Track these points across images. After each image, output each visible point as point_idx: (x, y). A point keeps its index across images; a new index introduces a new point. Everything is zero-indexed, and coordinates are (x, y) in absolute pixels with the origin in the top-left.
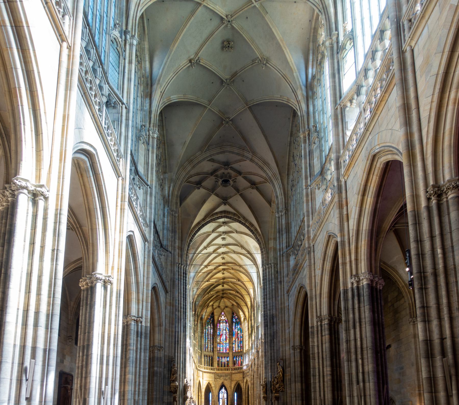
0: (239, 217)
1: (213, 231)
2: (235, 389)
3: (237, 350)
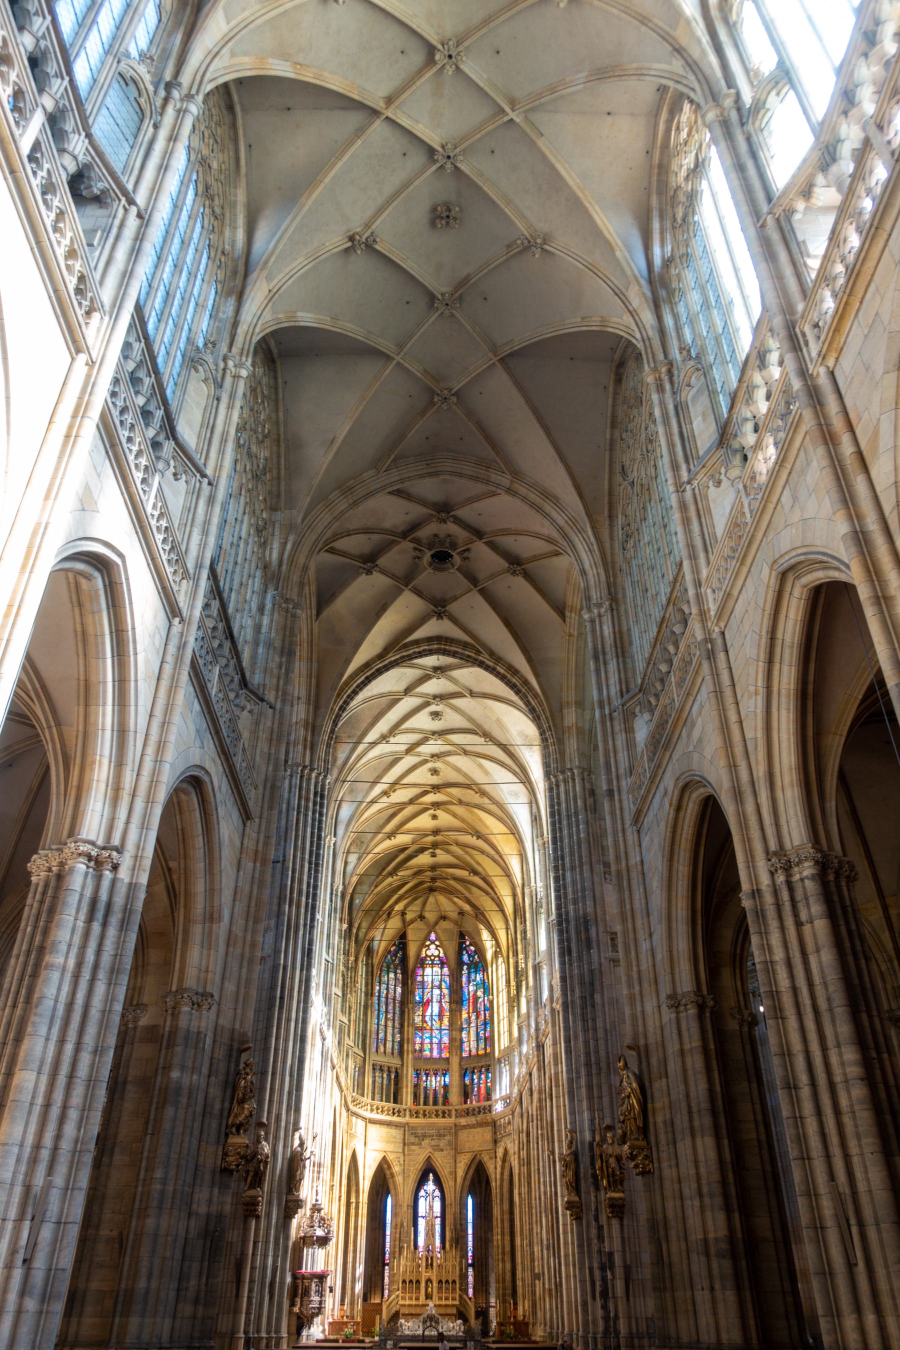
0: (478, 652)
1: (408, 691)
2: (467, 1183)
3: (474, 1051)
